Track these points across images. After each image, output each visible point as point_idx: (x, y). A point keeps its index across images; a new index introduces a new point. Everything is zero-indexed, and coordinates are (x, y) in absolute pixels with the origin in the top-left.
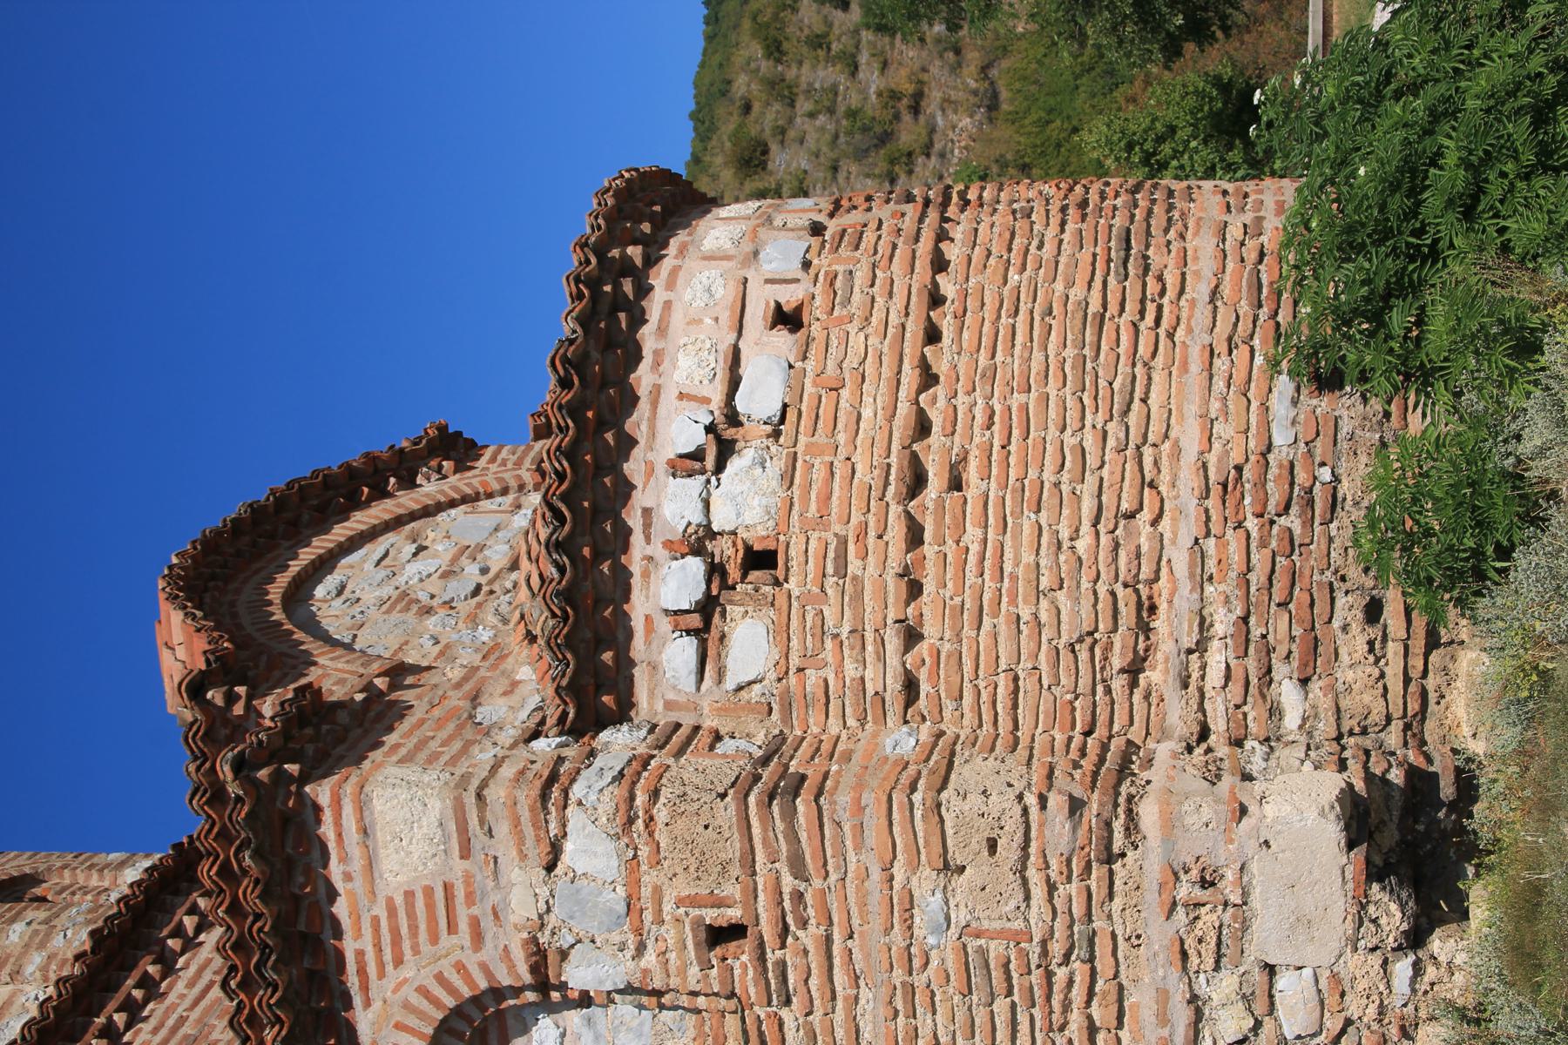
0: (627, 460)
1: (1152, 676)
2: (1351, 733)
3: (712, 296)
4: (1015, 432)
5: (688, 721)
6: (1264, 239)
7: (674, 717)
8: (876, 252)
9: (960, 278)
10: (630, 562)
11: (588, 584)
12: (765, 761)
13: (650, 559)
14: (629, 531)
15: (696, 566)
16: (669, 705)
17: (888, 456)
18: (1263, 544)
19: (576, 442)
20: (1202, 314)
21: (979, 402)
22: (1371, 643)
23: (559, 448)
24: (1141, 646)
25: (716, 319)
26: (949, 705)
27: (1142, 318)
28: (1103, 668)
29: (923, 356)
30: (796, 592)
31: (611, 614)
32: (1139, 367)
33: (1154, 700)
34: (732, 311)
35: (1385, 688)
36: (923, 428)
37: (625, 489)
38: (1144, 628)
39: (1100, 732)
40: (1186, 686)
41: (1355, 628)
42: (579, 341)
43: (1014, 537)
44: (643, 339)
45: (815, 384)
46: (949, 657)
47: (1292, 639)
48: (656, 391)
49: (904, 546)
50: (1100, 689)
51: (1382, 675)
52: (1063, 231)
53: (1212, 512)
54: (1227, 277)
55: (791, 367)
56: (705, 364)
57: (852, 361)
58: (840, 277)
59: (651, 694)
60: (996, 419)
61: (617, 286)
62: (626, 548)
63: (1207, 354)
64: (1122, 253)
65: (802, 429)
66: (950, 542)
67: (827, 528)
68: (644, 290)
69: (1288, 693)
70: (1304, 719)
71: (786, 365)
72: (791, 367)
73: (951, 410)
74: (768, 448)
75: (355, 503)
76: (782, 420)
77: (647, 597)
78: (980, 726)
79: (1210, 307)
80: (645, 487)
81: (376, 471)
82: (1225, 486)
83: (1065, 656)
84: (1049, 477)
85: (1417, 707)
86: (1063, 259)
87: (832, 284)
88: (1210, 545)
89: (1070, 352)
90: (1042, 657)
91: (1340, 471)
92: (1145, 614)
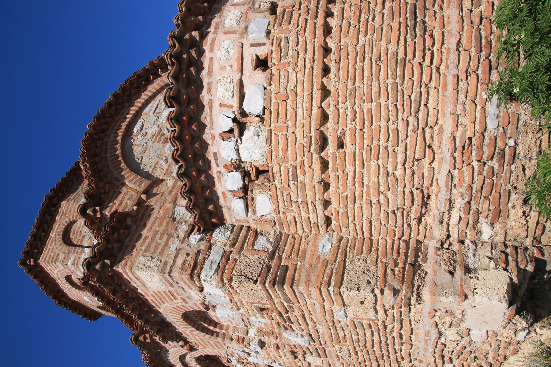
0: (204, 134)
1: (428, 219)
2: (510, 240)
3: (229, 54)
4: (366, 123)
5: (244, 224)
6: (482, 8)
7: (240, 224)
8: (298, 26)
10: (212, 172)
11: (197, 185)
12: (272, 257)
13: (220, 172)
14: (210, 162)
15: (237, 175)
16: (237, 221)
17: (310, 133)
18: (480, 173)
19: (181, 131)
20: (453, 55)
21: (349, 107)
22: (524, 213)
23: (174, 137)
24: (423, 211)
25: (232, 66)
26: (344, 229)
27: (424, 60)
28: (407, 219)
29: (322, 83)
30: (278, 186)
31: (209, 194)
32: (423, 87)
33: (428, 228)
34: (238, 62)
35: (528, 227)
36: (325, 117)
37: (205, 146)
38: (425, 204)
39: (405, 237)
40: (442, 223)
41: (518, 207)
42: (174, 88)
43: (367, 170)
44: (203, 78)
45: (276, 98)
46: (342, 213)
47: (489, 210)
48: (211, 102)
49: (320, 172)
50: (406, 225)
51: (527, 222)
52: (384, 8)
53: (457, 159)
54: (465, 34)
55: (265, 89)
56: (228, 89)
57: (291, 86)
58: (283, 41)
59: (230, 217)
60: (357, 115)
61: (189, 54)
62: (210, 168)
63: (456, 80)
64: (413, 22)
65: (272, 119)
66: (340, 171)
67: (287, 162)
68: (201, 53)
69: (485, 227)
70: (491, 237)
71: (263, 89)
72: (265, 89)
73: (336, 111)
74: (259, 126)
75: (149, 82)
76: (264, 114)
77: (221, 186)
78: (357, 235)
79: (457, 52)
80: (212, 144)
81: (155, 67)
82: (463, 147)
83: (391, 216)
84: (382, 143)
85: (540, 233)
86: (385, 27)
87: (279, 45)
88: (456, 173)
89: (390, 81)
90: (381, 215)
91: (519, 141)
92: (425, 200)
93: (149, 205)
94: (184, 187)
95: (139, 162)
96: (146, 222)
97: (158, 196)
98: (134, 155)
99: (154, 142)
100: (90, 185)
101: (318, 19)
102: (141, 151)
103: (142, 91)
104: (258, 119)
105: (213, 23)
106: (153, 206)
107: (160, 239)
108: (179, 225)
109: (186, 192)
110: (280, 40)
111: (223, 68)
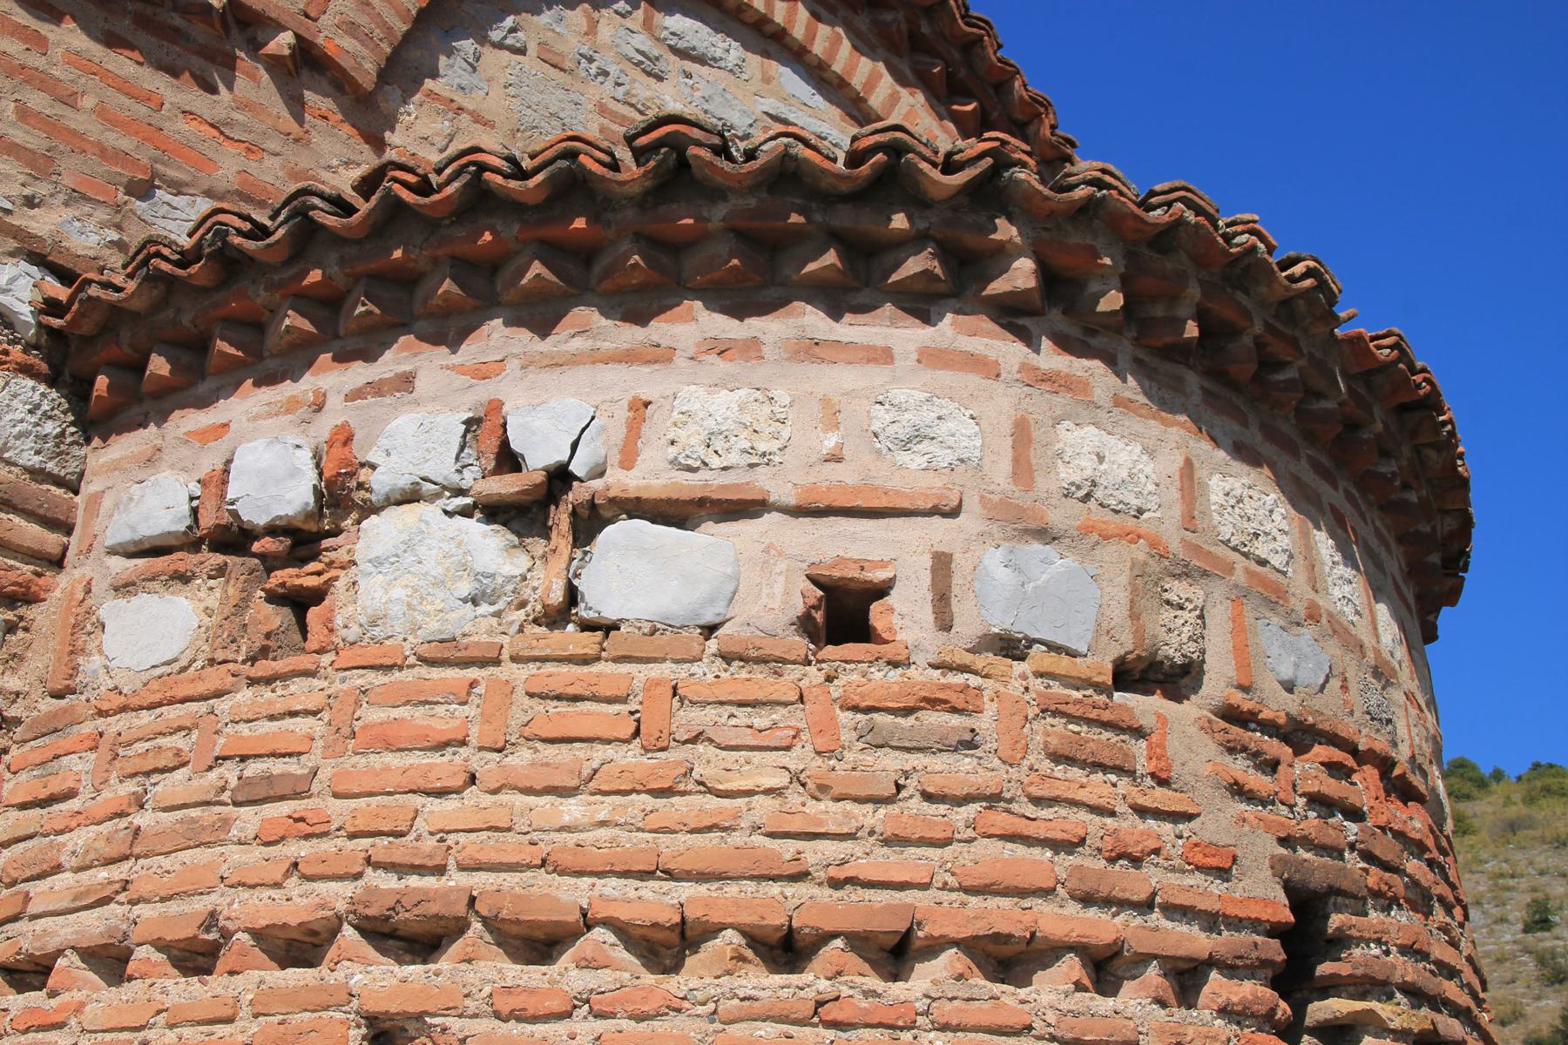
0: (507, 324)
3: (906, 444)
8: (1037, 801)
9: (945, 1011)
13: (319, 407)
14: (369, 356)
17: (462, 868)
23: (483, 167)
25: (835, 458)
29: (714, 931)
30: (223, 705)
31: (222, 354)
34: (857, 491)
42: (726, 166)
44: (789, 315)
48: (660, 356)
49: (263, 923)
55: (710, 630)
56: (718, 444)
57: (708, 762)
58: (955, 720)
59: (115, 466)
62: (343, 358)
65: (550, 668)
67: (330, 751)
71: (709, 618)
73: (555, 1005)
74: (523, 605)
77: (255, 418)
80: (460, 369)
87: (933, 703)
93: (233, 68)
94: (247, 226)
95: (495, 35)
96: (132, 48)
97: (285, 113)
98: (537, 11)
99: (602, 110)
101: (1073, 908)
102: (559, 47)
103: (896, 61)
104: (557, 596)
105: (1092, 370)
106: (230, 88)
107: (24, 113)
108: (102, 214)
109: (222, 235)
110: (960, 704)
111: (831, 416)
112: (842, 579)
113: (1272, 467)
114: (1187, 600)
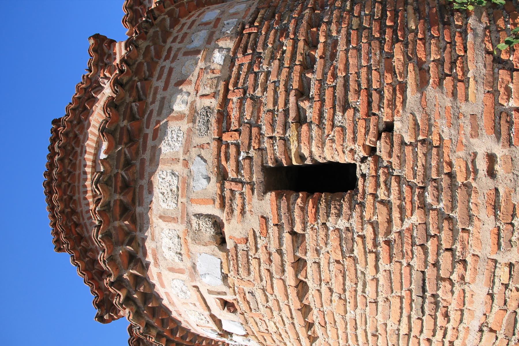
8: (261, 280)
100: (94, 292)
101: (286, 274)
103: (86, 126)
112: (222, 305)
113: (150, 177)
114: (196, 223)
